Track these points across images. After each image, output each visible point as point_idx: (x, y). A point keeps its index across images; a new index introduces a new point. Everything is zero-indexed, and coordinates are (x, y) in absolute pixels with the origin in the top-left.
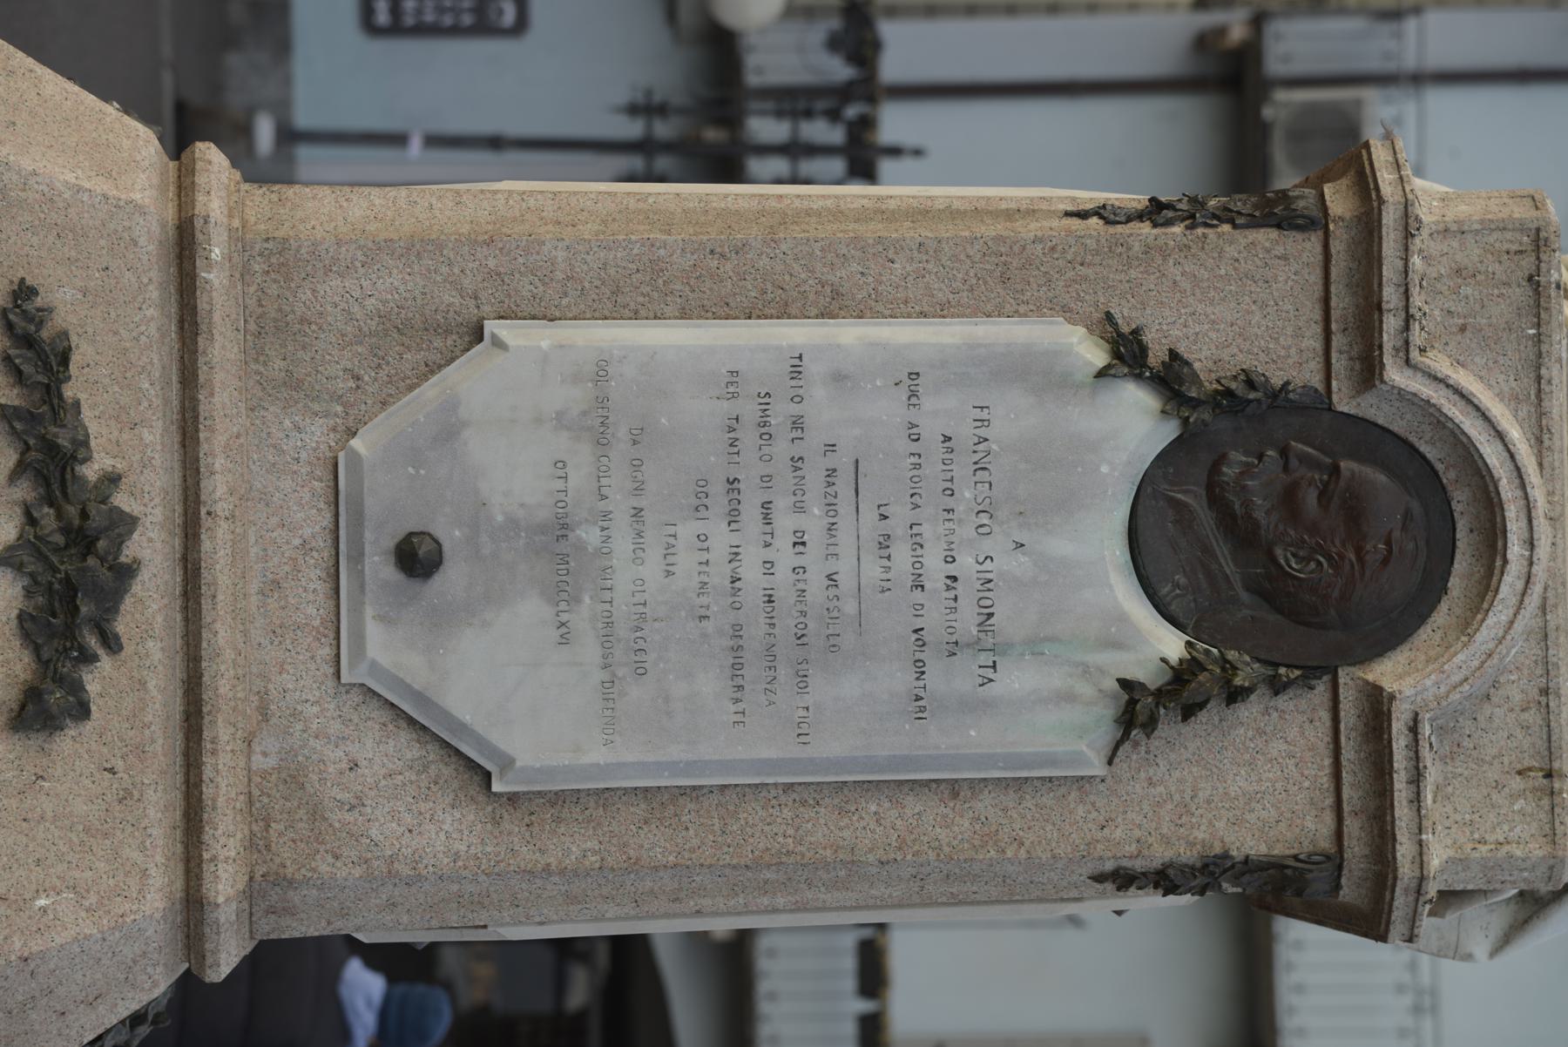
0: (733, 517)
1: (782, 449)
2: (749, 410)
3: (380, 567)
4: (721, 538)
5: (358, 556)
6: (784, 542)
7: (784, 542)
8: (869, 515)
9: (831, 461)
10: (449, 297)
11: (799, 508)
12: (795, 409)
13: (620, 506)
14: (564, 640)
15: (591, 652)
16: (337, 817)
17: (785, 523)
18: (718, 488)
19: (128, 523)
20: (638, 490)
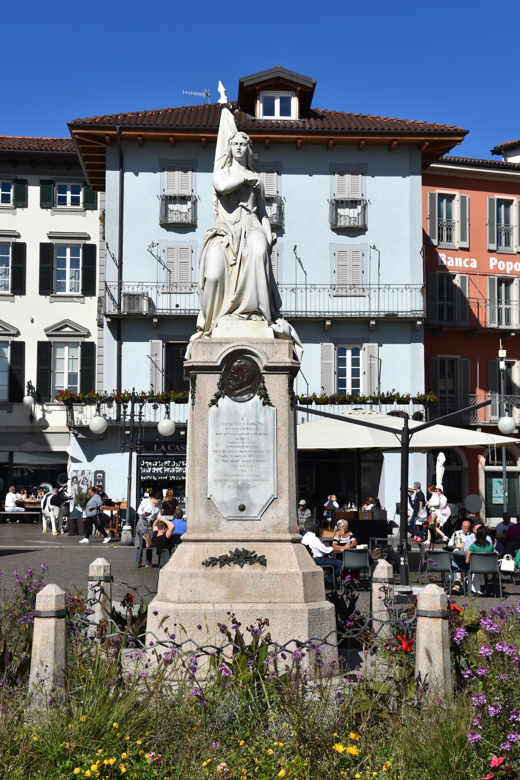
0: (237, 461)
1: (227, 454)
2: (222, 458)
3: (244, 514)
4: (240, 463)
5: (242, 517)
6: (241, 454)
7: (241, 454)
8: (237, 441)
9: (229, 447)
10: (204, 503)
11: (236, 451)
12: (221, 452)
13: (235, 478)
14: (255, 487)
15: (257, 483)
16: (280, 520)
17: (238, 454)
18: (233, 463)
19: (237, 550)
20: (233, 475)
